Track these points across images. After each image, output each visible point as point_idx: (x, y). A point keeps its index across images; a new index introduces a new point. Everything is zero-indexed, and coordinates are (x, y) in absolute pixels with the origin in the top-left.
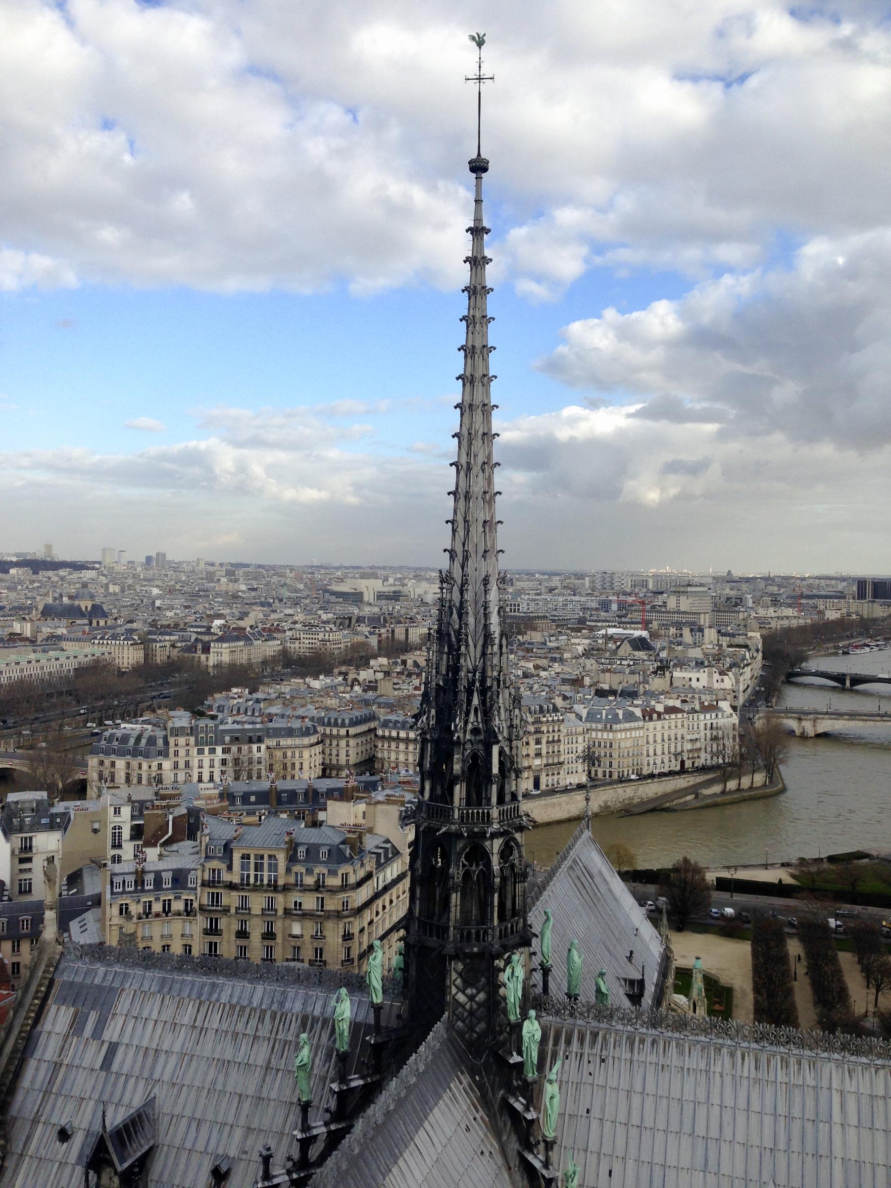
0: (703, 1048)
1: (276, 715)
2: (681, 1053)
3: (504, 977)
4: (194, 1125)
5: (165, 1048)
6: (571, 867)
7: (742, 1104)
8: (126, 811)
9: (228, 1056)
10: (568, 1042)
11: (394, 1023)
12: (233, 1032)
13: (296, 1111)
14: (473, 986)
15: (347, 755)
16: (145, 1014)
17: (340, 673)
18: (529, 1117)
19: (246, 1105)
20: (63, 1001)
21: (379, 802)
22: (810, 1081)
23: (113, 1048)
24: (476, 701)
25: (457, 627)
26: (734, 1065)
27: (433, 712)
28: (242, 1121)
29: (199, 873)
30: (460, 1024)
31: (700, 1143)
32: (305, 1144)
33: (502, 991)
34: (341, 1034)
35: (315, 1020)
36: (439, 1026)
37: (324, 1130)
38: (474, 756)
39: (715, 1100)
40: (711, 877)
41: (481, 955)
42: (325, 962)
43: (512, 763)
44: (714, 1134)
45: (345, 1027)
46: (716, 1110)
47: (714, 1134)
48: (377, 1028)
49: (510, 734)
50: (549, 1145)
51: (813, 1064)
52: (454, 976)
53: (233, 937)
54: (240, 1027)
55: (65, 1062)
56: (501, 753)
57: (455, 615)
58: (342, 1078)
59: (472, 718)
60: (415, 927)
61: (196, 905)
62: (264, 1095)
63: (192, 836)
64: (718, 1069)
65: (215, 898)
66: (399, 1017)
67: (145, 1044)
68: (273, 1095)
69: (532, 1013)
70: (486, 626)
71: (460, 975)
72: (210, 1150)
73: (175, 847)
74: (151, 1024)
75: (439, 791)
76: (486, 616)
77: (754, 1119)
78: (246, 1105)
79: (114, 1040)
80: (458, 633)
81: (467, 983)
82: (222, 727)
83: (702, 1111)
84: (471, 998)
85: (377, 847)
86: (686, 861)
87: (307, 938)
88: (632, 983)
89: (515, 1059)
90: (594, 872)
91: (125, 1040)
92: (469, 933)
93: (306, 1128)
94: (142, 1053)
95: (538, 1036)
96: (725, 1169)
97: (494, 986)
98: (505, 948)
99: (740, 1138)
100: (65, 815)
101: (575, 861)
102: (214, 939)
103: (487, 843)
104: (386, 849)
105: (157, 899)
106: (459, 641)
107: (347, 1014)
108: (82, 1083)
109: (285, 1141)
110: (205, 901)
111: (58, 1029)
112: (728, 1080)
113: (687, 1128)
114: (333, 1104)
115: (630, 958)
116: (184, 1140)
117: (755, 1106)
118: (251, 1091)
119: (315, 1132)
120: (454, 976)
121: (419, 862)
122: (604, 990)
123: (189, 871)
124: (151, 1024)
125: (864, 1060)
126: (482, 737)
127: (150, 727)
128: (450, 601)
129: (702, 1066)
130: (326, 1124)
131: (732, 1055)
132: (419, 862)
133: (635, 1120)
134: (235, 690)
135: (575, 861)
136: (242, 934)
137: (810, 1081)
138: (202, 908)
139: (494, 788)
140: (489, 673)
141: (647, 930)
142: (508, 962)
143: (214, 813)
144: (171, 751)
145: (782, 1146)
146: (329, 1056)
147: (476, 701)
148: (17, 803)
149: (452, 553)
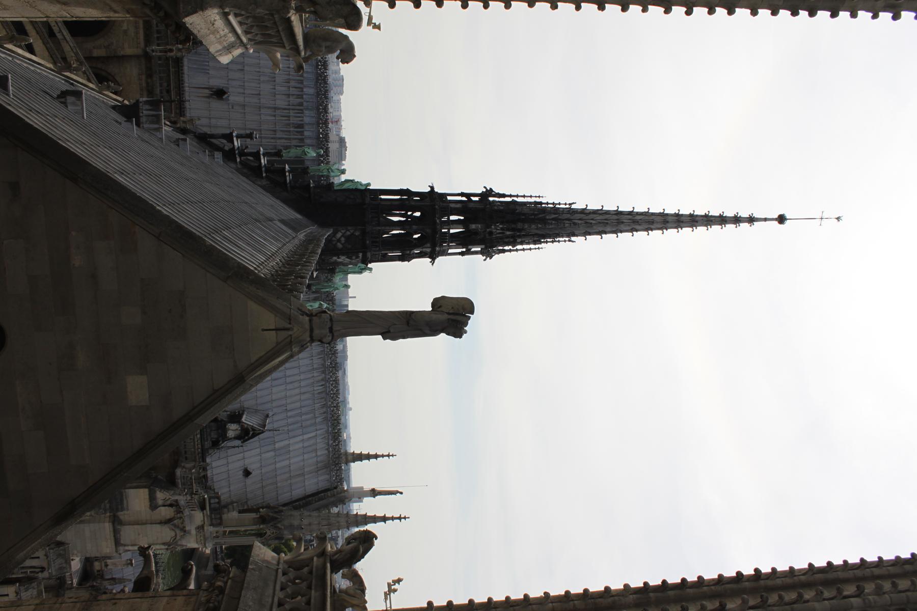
2: (319, 354)
4: (240, 67)
7: (303, 390)
12: (289, 79)
22: (318, 420)
24: (508, 233)
35: (302, 133)
39: (302, 377)
44: (288, 380)
47: (288, 380)
51: (326, 419)
57: (554, 216)
62: (263, 111)
64: (315, 375)
71: (352, 234)
77: (298, 397)
81: (348, 239)
83: (296, 371)
84: (339, 240)
96: (275, 390)
112: (311, 381)
117: (303, 397)
118: (263, 101)
126: (487, 236)
129: (315, 366)
131: (322, 380)
137: (318, 420)
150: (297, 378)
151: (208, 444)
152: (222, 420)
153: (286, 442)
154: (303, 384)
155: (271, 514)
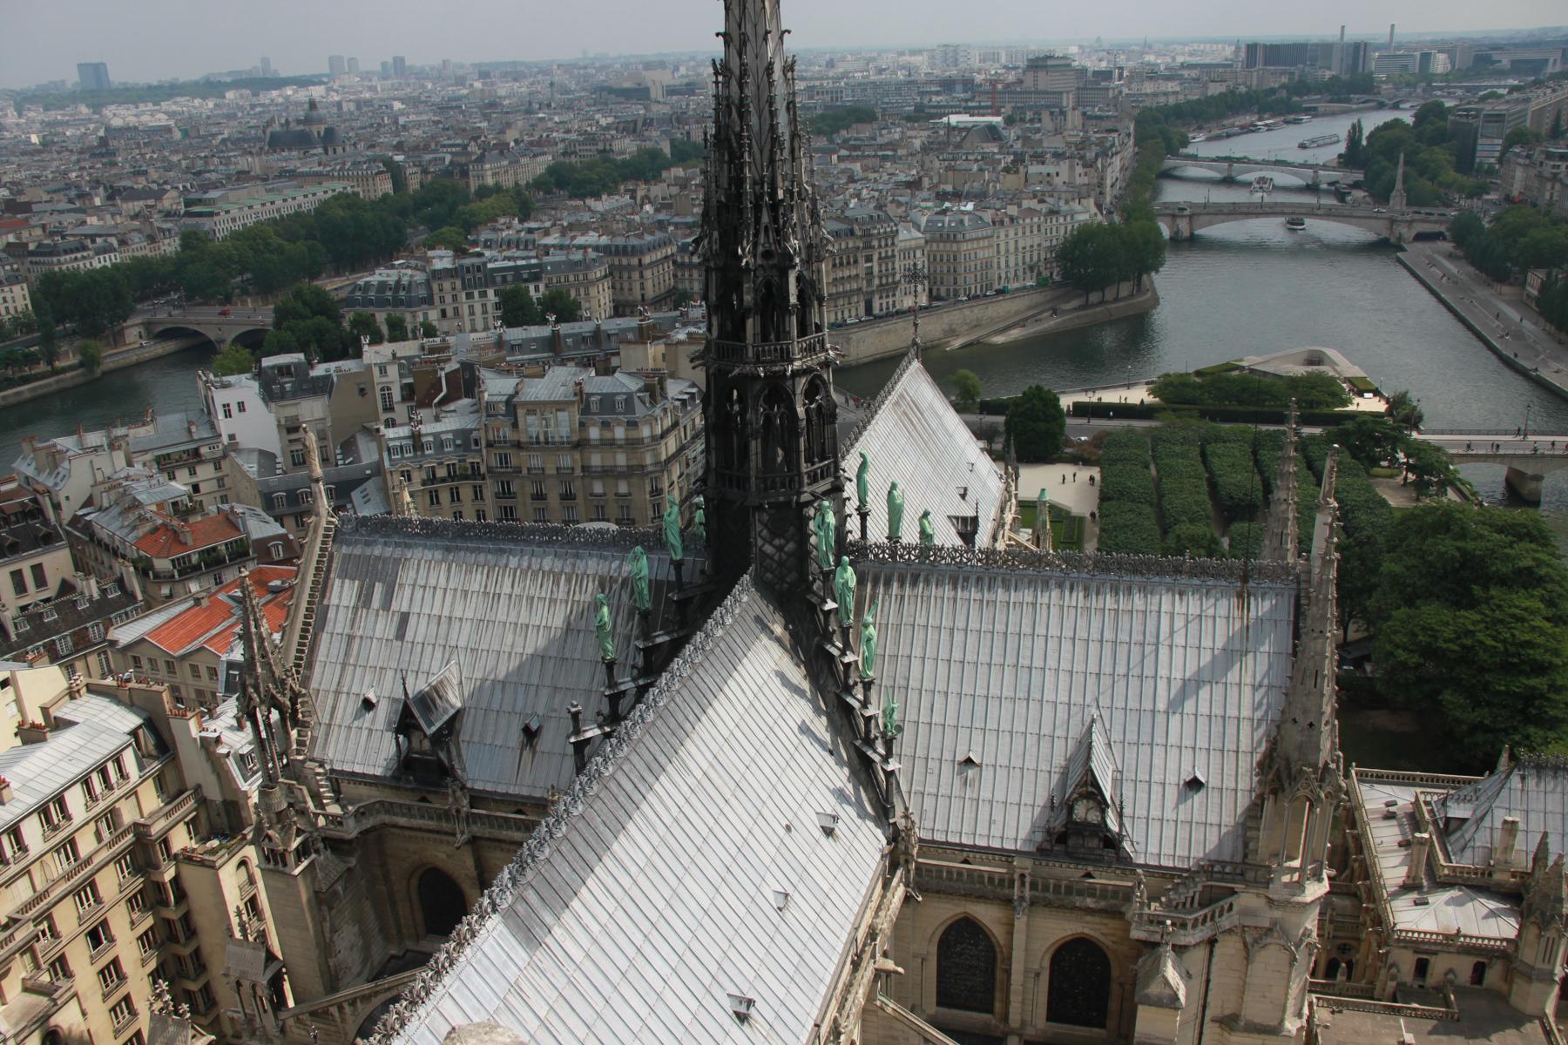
0: (1030, 582)
1: (553, 246)
3: (812, 525)
5: (458, 613)
6: (897, 403)
7: (1068, 633)
8: (393, 371)
9: (523, 619)
10: (888, 584)
11: (698, 580)
13: (601, 672)
14: (779, 536)
15: (642, 288)
16: (432, 582)
17: (627, 191)
18: (846, 660)
19: (550, 665)
20: (344, 575)
21: (680, 343)
23: (404, 618)
24: (765, 219)
25: (738, 129)
26: (1062, 598)
27: (716, 234)
28: (547, 682)
29: (482, 433)
30: (769, 575)
31: (1023, 674)
32: (614, 699)
33: (813, 540)
34: (641, 593)
36: (746, 577)
37: (632, 685)
38: (768, 285)
40: (1066, 402)
41: (788, 503)
42: (632, 522)
43: (814, 288)
44: (1038, 663)
45: (644, 585)
46: (1039, 643)
48: (679, 585)
49: (809, 255)
50: (867, 686)
52: (759, 527)
53: (529, 500)
54: (534, 591)
55: (360, 633)
56: (798, 279)
57: (735, 114)
58: (646, 635)
59: (762, 239)
60: (712, 478)
61: (483, 469)
62: (567, 655)
63: (469, 393)
65: (504, 459)
66: (702, 572)
67: (436, 611)
68: (577, 656)
69: (846, 558)
70: (773, 128)
71: (766, 526)
72: (518, 710)
73: (452, 407)
74: (439, 593)
75: (729, 326)
76: (773, 115)
78: (550, 665)
79: (404, 609)
80: (739, 137)
81: (775, 534)
82: (490, 266)
84: (780, 549)
85: (681, 393)
86: (1039, 388)
87: (611, 496)
88: (964, 519)
89: (830, 605)
90: (923, 406)
91: (416, 609)
92: (774, 482)
93: (612, 684)
94: (435, 621)
95: (853, 583)
96: (1049, 696)
97: (803, 536)
98: (816, 497)
99: (1065, 665)
100: (326, 378)
101: (901, 396)
102: (508, 503)
103: (789, 383)
104: (692, 395)
105: (441, 464)
106: (741, 146)
107: (645, 572)
108: (376, 654)
109: (594, 698)
110: (494, 462)
111: (344, 603)
112: (1054, 611)
113: (1010, 660)
114: (640, 661)
115: (963, 496)
116: (490, 703)
117: (1082, 634)
119: (622, 688)
120: (759, 527)
121: (711, 409)
122: (929, 531)
123: (471, 431)
124: (439, 593)
125: (1196, 581)
127: (409, 272)
128: (728, 98)
130: (634, 680)
132: (711, 409)
133: (957, 655)
134: (502, 220)
135: (901, 396)
136: (539, 497)
138: (490, 470)
139: (794, 319)
140: (780, 183)
141: (985, 464)
142: (819, 509)
143: (490, 365)
144: (436, 298)
145: (1107, 669)
146: (631, 615)
147: (765, 219)
148: (273, 367)
149: (726, 36)
150: (1042, 640)
151: (1109, 854)
152: (1065, 826)
153: (1162, 685)
154: (1054, 631)
155: (1270, 777)
